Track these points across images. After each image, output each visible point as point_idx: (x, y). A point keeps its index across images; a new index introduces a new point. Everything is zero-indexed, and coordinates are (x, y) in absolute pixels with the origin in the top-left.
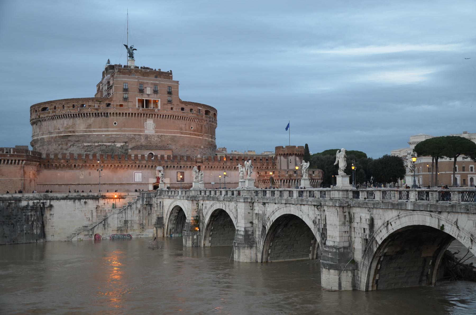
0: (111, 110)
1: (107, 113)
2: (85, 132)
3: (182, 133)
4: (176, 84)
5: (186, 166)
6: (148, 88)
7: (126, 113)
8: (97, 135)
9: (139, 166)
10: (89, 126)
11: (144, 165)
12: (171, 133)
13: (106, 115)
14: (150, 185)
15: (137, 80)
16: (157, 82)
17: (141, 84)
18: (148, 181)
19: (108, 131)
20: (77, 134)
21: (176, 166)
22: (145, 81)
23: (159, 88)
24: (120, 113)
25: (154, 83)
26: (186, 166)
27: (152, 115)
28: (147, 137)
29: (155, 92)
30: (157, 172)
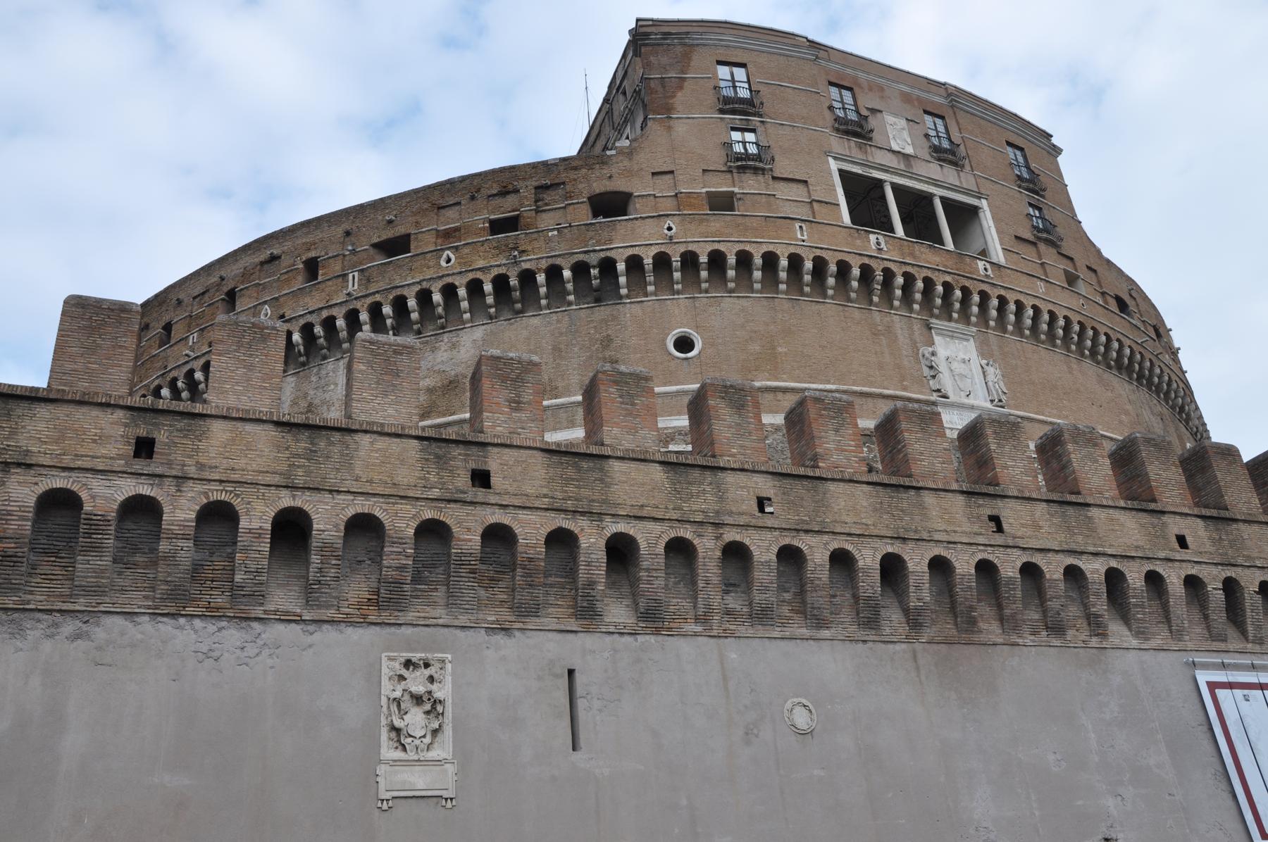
7: (770, 260)
13: (598, 281)
24: (717, 260)
25: (919, 99)
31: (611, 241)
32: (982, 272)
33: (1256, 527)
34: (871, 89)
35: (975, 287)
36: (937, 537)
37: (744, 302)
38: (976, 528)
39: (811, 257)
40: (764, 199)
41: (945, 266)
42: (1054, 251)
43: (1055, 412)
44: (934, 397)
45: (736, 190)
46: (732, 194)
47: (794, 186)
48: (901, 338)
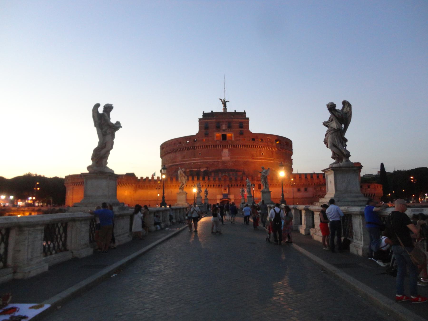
0: (197, 144)
2: (182, 161)
3: (253, 159)
4: (247, 120)
6: (223, 125)
8: (188, 163)
9: (208, 186)
10: (184, 157)
11: (212, 185)
13: (194, 148)
15: (214, 120)
19: (195, 160)
20: (177, 163)
21: (239, 185)
27: (227, 145)
28: (224, 162)
29: (229, 127)
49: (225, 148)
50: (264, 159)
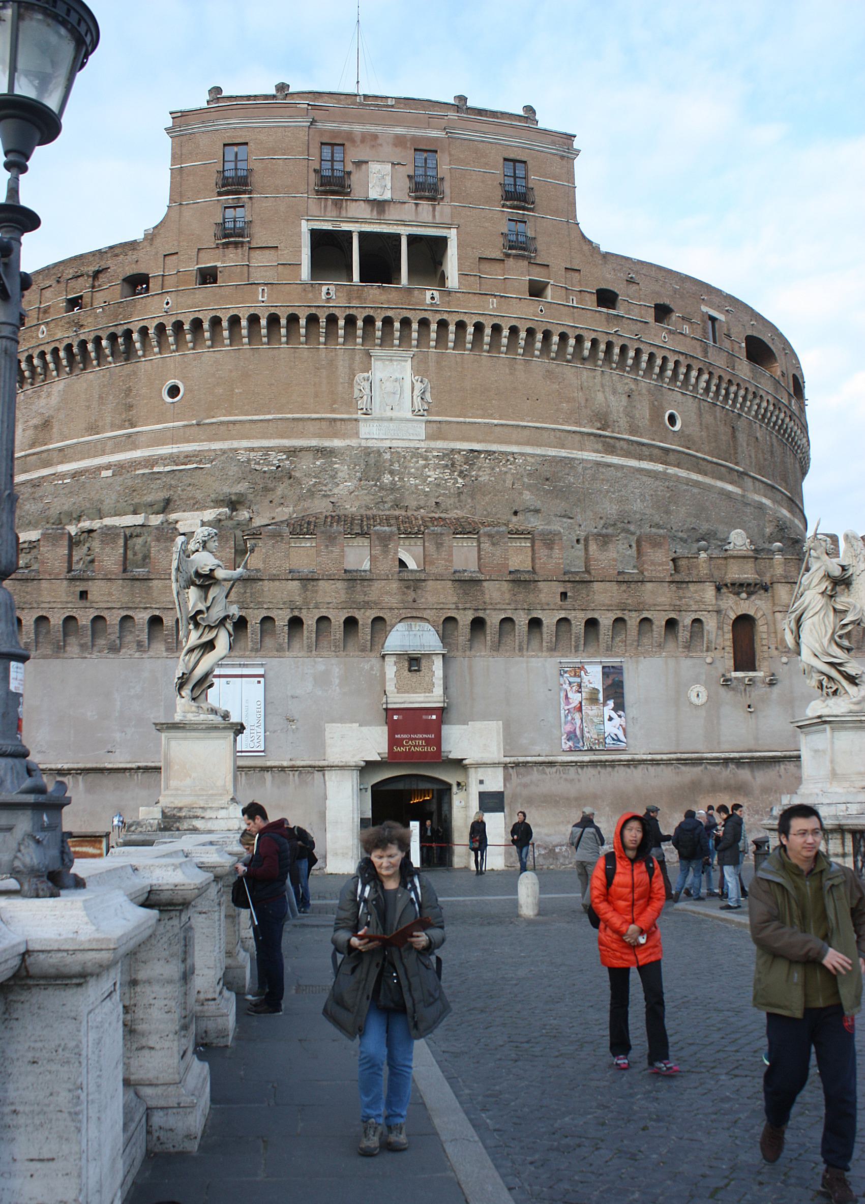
0: (151, 311)
1: (128, 334)
5: (633, 619)
6: (374, 167)
7: (235, 321)
8: (75, 475)
11: (282, 618)
12: (536, 437)
13: (123, 345)
14: (332, 778)
16: (434, 134)
17: (334, 144)
18: (319, 744)
19: (131, 442)
21: (549, 620)
22: (358, 128)
23: (444, 169)
24: (197, 324)
25: (414, 139)
26: (633, 619)
27: (406, 322)
28: (372, 463)
30: (391, 669)
31: (131, 315)
32: (428, 301)
33: (277, 583)
34: (363, 141)
35: (415, 317)
36: (43, 605)
37: (217, 355)
38: (69, 599)
39: (266, 315)
40: (238, 269)
41: (388, 302)
42: (526, 263)
43: (480, 412)
44: (359, 415)
45: (219, 264)
46: (216, 267)
47: (267, 252)
48: (341, 368)
49: (386, 341)
50: (682, 460)
